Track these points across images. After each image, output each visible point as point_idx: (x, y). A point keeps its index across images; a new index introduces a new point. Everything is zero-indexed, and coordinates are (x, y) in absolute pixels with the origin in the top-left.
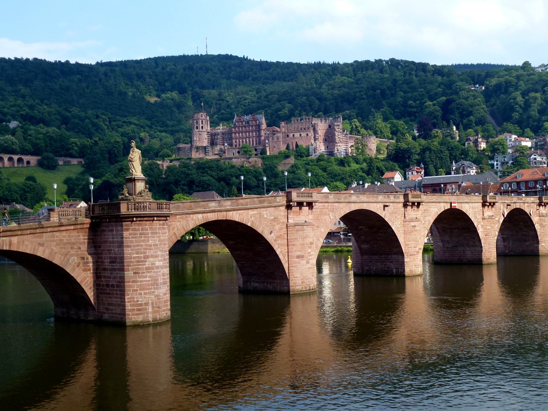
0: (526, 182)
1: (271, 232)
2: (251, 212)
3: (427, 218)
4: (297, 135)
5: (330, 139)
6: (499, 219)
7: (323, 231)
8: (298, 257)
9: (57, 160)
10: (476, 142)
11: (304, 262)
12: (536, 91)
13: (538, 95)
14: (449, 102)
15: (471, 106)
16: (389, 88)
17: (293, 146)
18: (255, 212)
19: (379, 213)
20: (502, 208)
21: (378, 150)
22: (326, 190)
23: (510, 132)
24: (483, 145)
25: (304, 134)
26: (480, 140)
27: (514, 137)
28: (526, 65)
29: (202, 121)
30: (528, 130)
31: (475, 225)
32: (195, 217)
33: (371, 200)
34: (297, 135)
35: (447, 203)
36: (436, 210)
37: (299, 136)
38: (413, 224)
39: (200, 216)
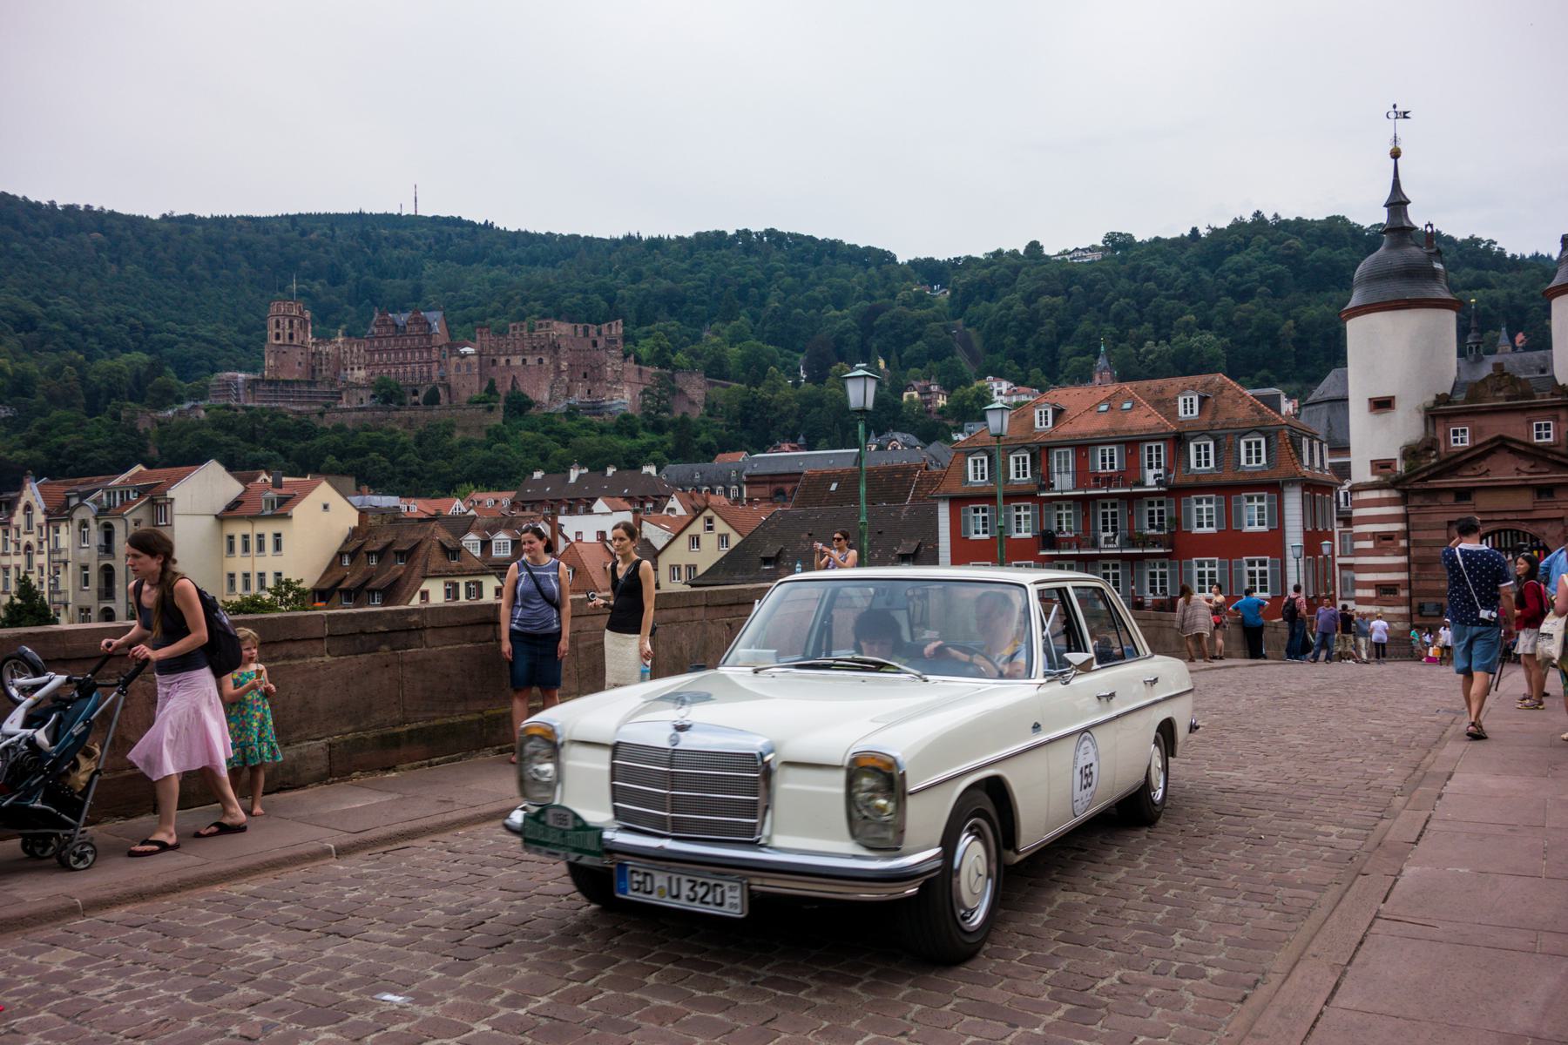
0: (1082, 447)
4: (516, 361)
5: (592, 374)
10: (925, 391)
12: (1054, 294)
13: (1059, 300)
14: (875, 312)
15: (921, 322)
16: (756, 284)
17: (504, 388)
21: (711, 407)
23: (1000, 375)
24: (942, 401)
25: (532, 361)
26: (934, 388)
27: (1005, 386)
28: (1034, 247)
29: (291, 323)
30: (1036, 371)
34: (516, 361)
37: (520, 363)
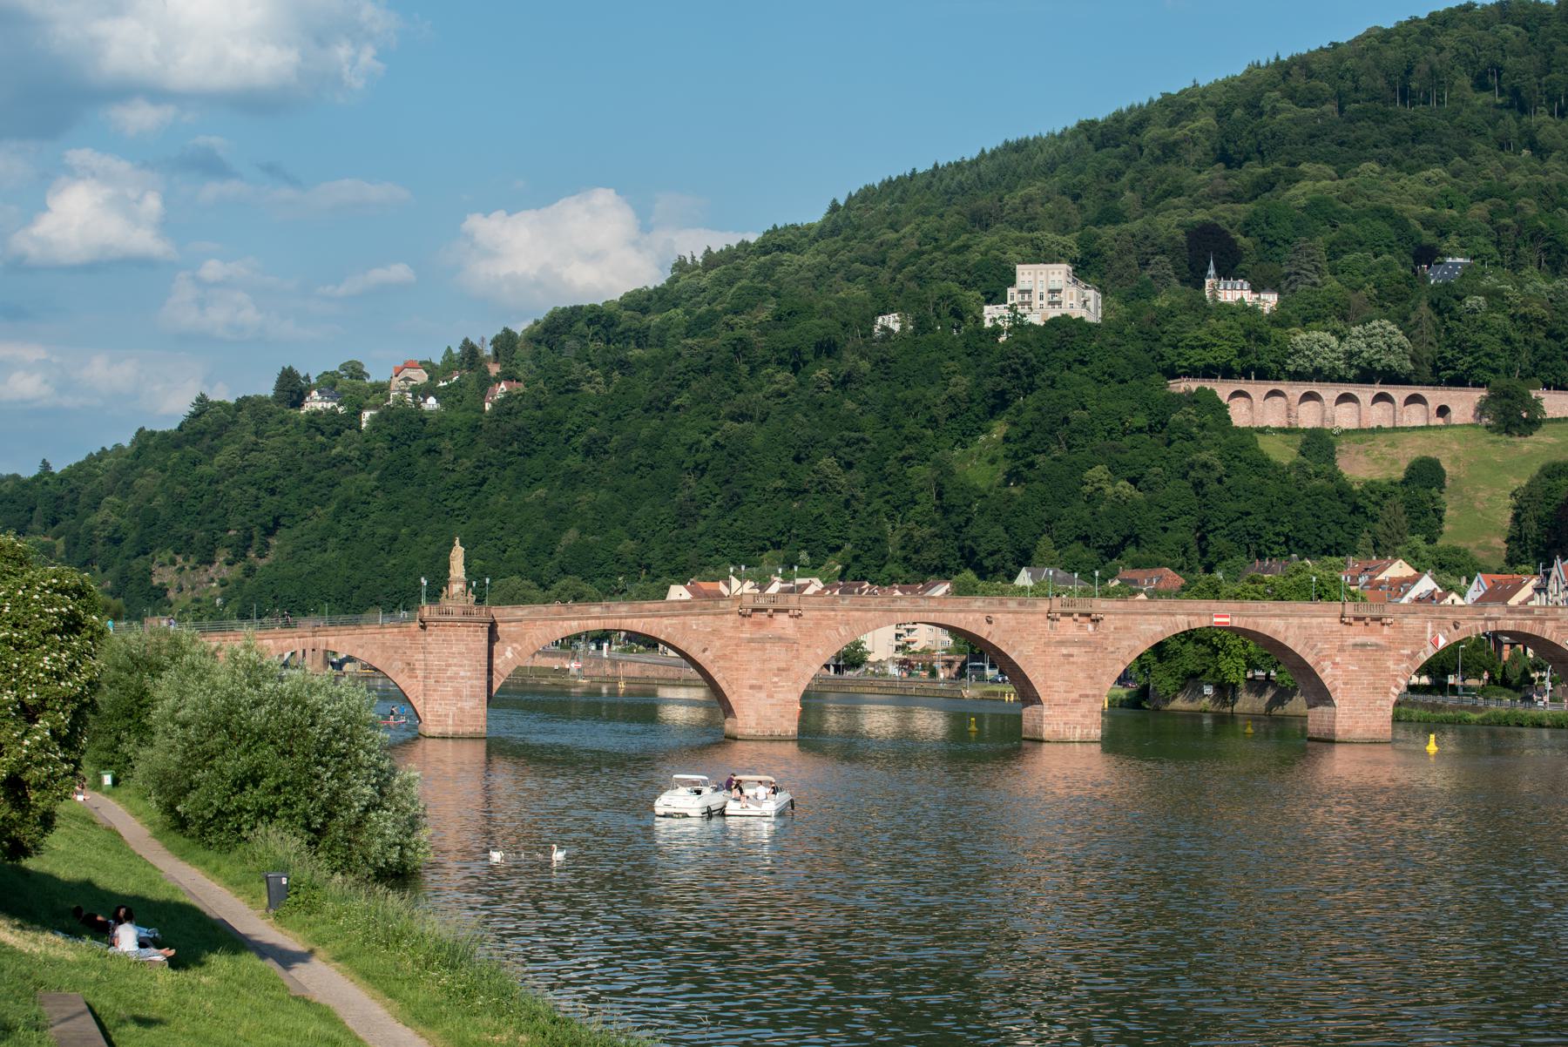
1: (705, 650)
2: (666, 621)
3: (1125, 643)
6: (1414, 654)
7: (819, 651)
8: (752, 687)
9: (1536, 404)
11: (763, 695)
18: (674, 621)
19: (973, 629)
20: (1429, 630)
22: (942, 589)
31: (1310, 660)
32: (566, 624)
33: (949, 608)
35: (1198, 614)
36: (1159, 628)
38: (1065, 651)
39: (575, 623)
